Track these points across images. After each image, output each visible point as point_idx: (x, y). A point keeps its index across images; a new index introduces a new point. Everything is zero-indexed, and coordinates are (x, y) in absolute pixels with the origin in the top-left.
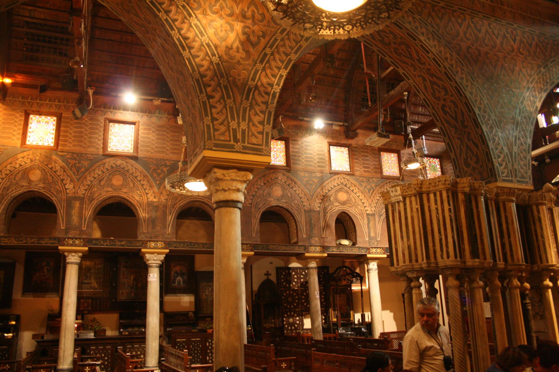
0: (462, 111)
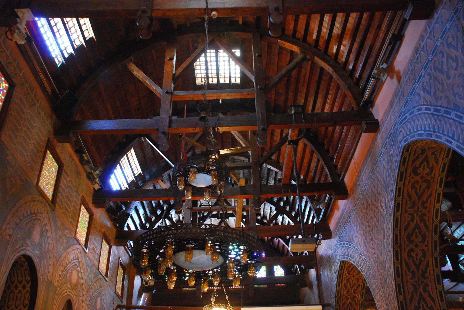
0: (428, 262)
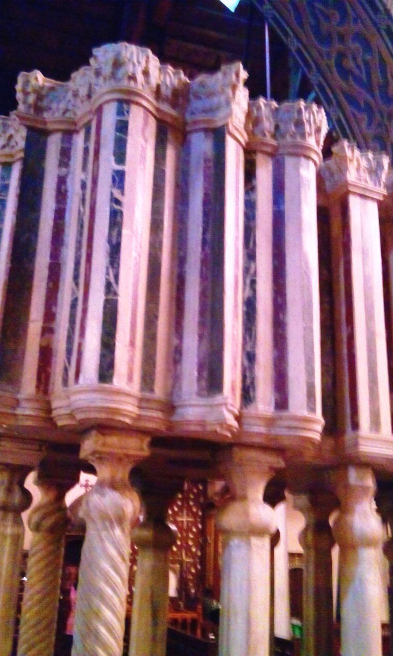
0: (380, 53)
